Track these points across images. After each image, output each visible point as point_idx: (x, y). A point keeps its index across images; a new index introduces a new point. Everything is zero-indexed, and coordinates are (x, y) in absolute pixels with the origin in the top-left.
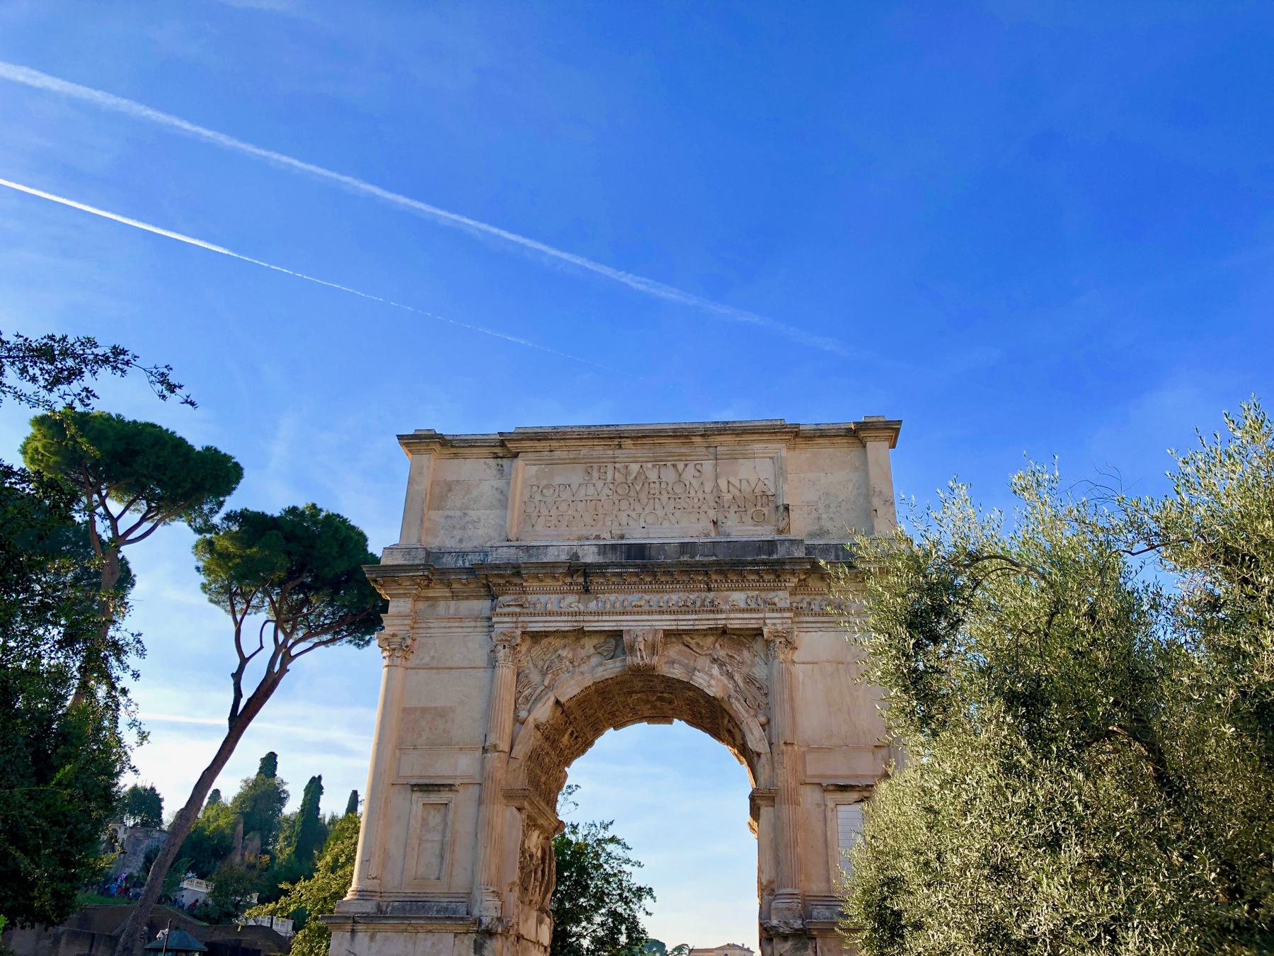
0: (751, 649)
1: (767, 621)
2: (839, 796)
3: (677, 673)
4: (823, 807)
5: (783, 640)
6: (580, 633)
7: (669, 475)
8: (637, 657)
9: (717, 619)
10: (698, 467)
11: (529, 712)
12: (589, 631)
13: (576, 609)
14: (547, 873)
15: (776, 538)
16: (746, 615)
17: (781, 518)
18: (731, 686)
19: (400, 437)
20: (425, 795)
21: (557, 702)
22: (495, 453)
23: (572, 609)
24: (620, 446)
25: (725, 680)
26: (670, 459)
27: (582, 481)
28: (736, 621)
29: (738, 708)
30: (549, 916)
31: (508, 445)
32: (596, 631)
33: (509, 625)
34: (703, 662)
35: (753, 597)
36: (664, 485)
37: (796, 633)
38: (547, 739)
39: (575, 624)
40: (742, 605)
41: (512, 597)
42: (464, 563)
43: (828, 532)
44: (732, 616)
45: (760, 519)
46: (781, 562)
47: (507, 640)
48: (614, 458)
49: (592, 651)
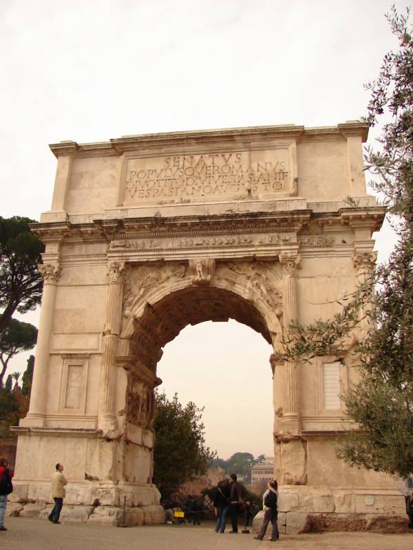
3: (223, 285)
7: (219, 161)
8: (197, 275)
10: (239, 156)
11: (131, 310)
12: (168, 261)
14: (150, 407)
15: (288, 198)
19: (51, 146)
20: (69, 360)
23: (157, 248)
25: (255, 289)
27: (163, 168)
29: (263, 307)
30: (152, 432)
31: (117, 147)
32: (172, 261)
33: (118, 258)
34: (243, 278)
36: (216, 168)
38: (145, 328)
39: (159, 257)
40: (267, 242)
44: (259, 249)
45: (279, 186)
48: (184, 152)
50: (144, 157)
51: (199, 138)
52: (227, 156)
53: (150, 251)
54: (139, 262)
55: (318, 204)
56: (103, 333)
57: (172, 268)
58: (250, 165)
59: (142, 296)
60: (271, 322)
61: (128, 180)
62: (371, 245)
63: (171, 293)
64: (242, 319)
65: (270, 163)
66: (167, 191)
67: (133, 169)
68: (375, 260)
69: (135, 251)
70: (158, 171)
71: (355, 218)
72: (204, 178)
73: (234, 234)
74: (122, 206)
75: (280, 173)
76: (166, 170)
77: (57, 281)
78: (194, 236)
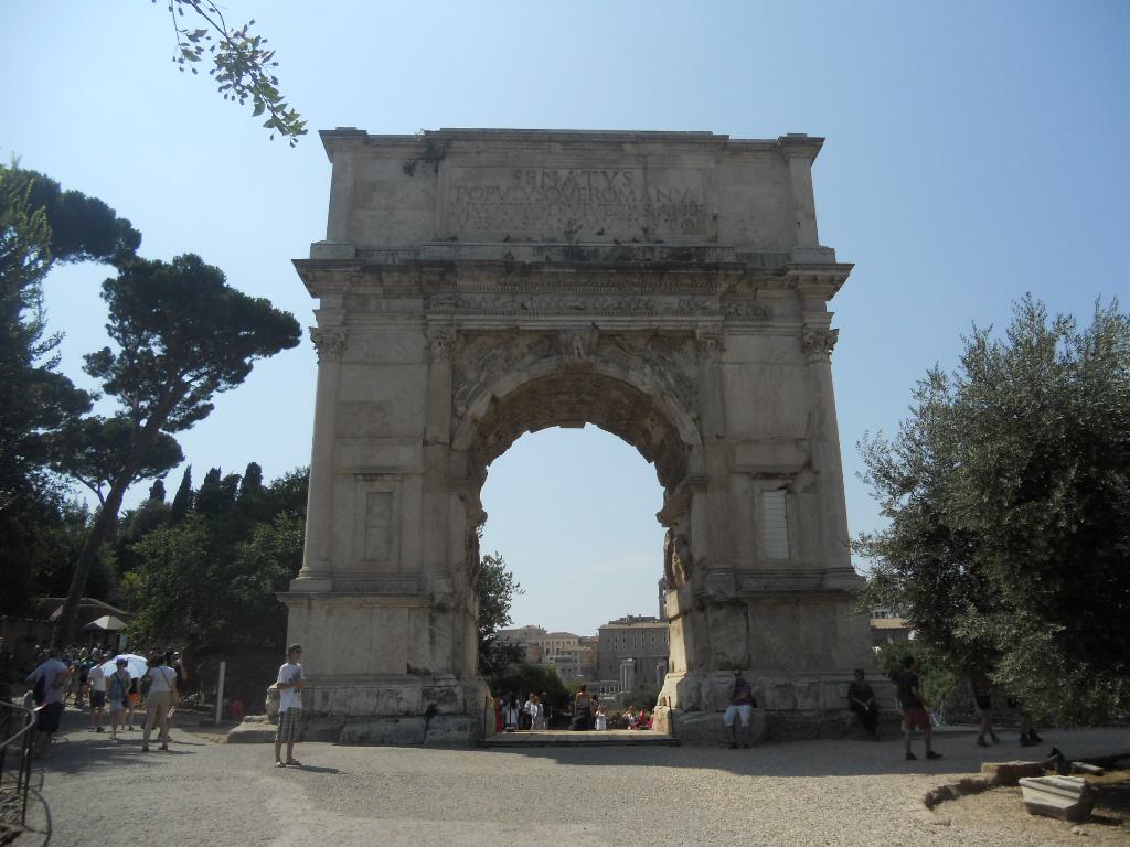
1: (700, 324)
2: (765, 483)
6: (514, 332)
7: (599, 182)
9: (650, 321)
10: (628, 175)
11: (467, 407)
12: (523, 331)
15: (708, 245)
16: (680, 318)
18: (662, 384)
21: (494, 400)
26: (601, 166)
28: (669, 323)
32: (530, 331)
36: (594, 192)
37: (726, 334)
40: (675, 307)
42: (394, 261)
44: (666, 318)
46: (716, 267)
47: (442, 338)
49: (526, 350)
51: (568, 142)
55: (749, 256)
56: (424, 440)
60: (685, 427)
62: (827, 321)
64: (610, 424)
68: (835, 342)
77: (341, 355)
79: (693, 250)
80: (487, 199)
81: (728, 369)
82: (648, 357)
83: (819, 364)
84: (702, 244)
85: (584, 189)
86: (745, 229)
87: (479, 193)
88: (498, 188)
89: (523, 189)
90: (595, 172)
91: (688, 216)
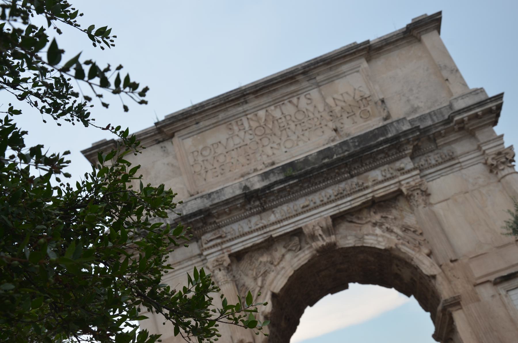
0: (397, 207)
1: (403, 182)
4: (498, 297)
5: (419, 191)
7: (289, 109)
8: (318, 240)
10: (308, 96)
13: (261, 225)
15: (386, 123)
17: (382, 110)
21: (274, 296)
22: (156, 140)
24: (246, 102)
25: (387, 235)
27: (228, 136)
29: (407, 250)
31: (165, 130)
34: (367, 228)
35: (385, 170)
36: (288, 118)
37: (426, 183)
39: (265, 235)
40: (380, 178)
41: (211, 233)
43: (418, 107)
44: (376, 188)
45: (367, 116)
47: (220, 265)
49: (283, 251)
50: (201, 131)
52: (295, 100)
53: (252, 232)
54: (242, 250)
57: (284, 243)
58: (325, 102)
59: (261, 287)
60: (424, 264)
61: (192, 163)
63: (296, 272)
65: (347, 93)
66: (242, 160)
67: (194, 149)
68: (514, 156)
69: (236, 238)
70: (224, 142)
71: (470, 118)
72: (280, 133)
73: (340, 182)
74: (198, 193)
75: (361, 100)
76: (232, 138)
78: (296, 199)
79: (376, 131)
80: (215, 152)
81: (438, 208)
82: (374, 221)
83: (507, 178)
84: (381, 124)
85: (280, 118)
86: (408, 101)
87: (208, 151)
88: (220, 142)
89: (238, 135)
90: (283, 104)
91: (362, 106)
